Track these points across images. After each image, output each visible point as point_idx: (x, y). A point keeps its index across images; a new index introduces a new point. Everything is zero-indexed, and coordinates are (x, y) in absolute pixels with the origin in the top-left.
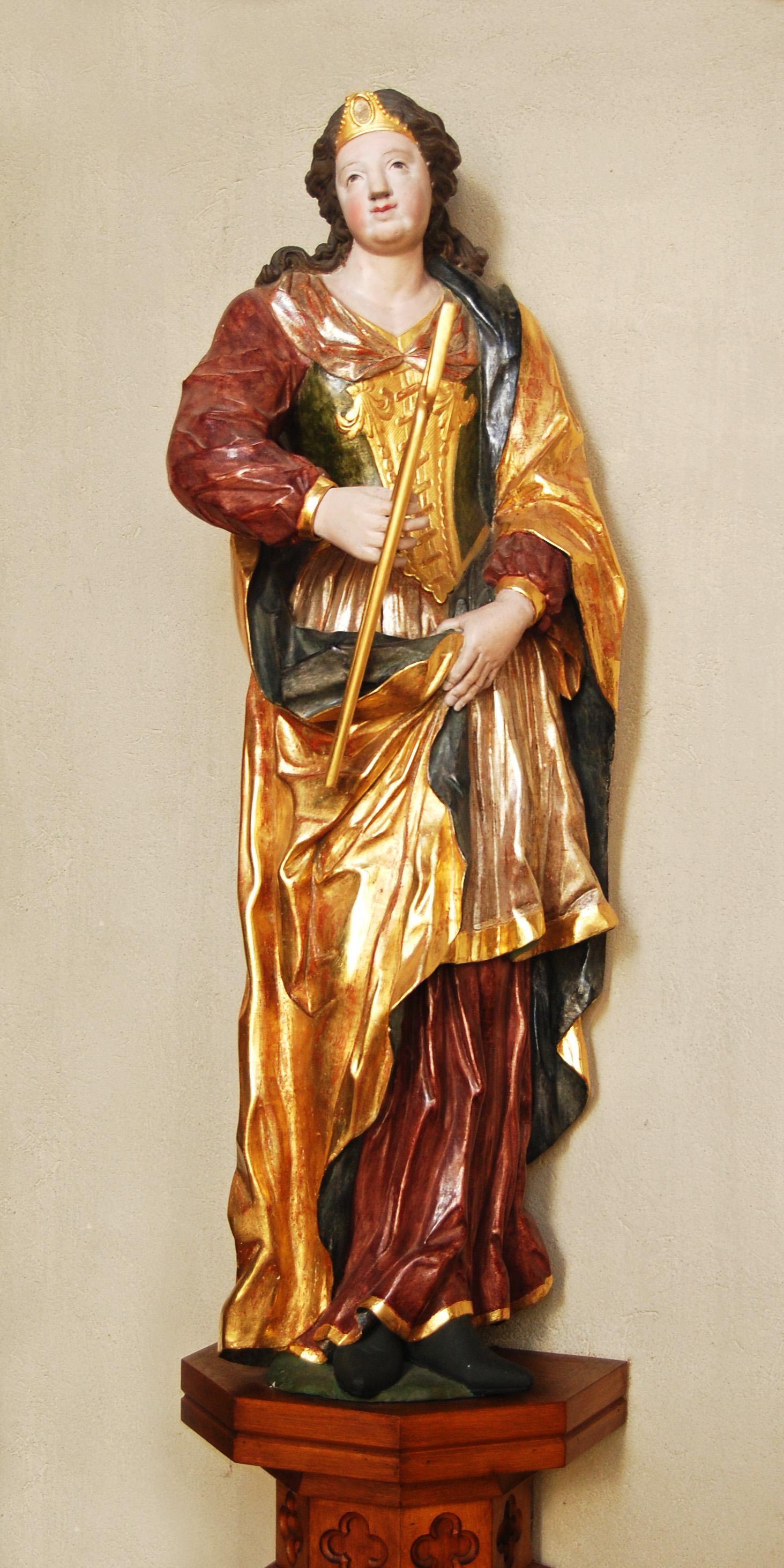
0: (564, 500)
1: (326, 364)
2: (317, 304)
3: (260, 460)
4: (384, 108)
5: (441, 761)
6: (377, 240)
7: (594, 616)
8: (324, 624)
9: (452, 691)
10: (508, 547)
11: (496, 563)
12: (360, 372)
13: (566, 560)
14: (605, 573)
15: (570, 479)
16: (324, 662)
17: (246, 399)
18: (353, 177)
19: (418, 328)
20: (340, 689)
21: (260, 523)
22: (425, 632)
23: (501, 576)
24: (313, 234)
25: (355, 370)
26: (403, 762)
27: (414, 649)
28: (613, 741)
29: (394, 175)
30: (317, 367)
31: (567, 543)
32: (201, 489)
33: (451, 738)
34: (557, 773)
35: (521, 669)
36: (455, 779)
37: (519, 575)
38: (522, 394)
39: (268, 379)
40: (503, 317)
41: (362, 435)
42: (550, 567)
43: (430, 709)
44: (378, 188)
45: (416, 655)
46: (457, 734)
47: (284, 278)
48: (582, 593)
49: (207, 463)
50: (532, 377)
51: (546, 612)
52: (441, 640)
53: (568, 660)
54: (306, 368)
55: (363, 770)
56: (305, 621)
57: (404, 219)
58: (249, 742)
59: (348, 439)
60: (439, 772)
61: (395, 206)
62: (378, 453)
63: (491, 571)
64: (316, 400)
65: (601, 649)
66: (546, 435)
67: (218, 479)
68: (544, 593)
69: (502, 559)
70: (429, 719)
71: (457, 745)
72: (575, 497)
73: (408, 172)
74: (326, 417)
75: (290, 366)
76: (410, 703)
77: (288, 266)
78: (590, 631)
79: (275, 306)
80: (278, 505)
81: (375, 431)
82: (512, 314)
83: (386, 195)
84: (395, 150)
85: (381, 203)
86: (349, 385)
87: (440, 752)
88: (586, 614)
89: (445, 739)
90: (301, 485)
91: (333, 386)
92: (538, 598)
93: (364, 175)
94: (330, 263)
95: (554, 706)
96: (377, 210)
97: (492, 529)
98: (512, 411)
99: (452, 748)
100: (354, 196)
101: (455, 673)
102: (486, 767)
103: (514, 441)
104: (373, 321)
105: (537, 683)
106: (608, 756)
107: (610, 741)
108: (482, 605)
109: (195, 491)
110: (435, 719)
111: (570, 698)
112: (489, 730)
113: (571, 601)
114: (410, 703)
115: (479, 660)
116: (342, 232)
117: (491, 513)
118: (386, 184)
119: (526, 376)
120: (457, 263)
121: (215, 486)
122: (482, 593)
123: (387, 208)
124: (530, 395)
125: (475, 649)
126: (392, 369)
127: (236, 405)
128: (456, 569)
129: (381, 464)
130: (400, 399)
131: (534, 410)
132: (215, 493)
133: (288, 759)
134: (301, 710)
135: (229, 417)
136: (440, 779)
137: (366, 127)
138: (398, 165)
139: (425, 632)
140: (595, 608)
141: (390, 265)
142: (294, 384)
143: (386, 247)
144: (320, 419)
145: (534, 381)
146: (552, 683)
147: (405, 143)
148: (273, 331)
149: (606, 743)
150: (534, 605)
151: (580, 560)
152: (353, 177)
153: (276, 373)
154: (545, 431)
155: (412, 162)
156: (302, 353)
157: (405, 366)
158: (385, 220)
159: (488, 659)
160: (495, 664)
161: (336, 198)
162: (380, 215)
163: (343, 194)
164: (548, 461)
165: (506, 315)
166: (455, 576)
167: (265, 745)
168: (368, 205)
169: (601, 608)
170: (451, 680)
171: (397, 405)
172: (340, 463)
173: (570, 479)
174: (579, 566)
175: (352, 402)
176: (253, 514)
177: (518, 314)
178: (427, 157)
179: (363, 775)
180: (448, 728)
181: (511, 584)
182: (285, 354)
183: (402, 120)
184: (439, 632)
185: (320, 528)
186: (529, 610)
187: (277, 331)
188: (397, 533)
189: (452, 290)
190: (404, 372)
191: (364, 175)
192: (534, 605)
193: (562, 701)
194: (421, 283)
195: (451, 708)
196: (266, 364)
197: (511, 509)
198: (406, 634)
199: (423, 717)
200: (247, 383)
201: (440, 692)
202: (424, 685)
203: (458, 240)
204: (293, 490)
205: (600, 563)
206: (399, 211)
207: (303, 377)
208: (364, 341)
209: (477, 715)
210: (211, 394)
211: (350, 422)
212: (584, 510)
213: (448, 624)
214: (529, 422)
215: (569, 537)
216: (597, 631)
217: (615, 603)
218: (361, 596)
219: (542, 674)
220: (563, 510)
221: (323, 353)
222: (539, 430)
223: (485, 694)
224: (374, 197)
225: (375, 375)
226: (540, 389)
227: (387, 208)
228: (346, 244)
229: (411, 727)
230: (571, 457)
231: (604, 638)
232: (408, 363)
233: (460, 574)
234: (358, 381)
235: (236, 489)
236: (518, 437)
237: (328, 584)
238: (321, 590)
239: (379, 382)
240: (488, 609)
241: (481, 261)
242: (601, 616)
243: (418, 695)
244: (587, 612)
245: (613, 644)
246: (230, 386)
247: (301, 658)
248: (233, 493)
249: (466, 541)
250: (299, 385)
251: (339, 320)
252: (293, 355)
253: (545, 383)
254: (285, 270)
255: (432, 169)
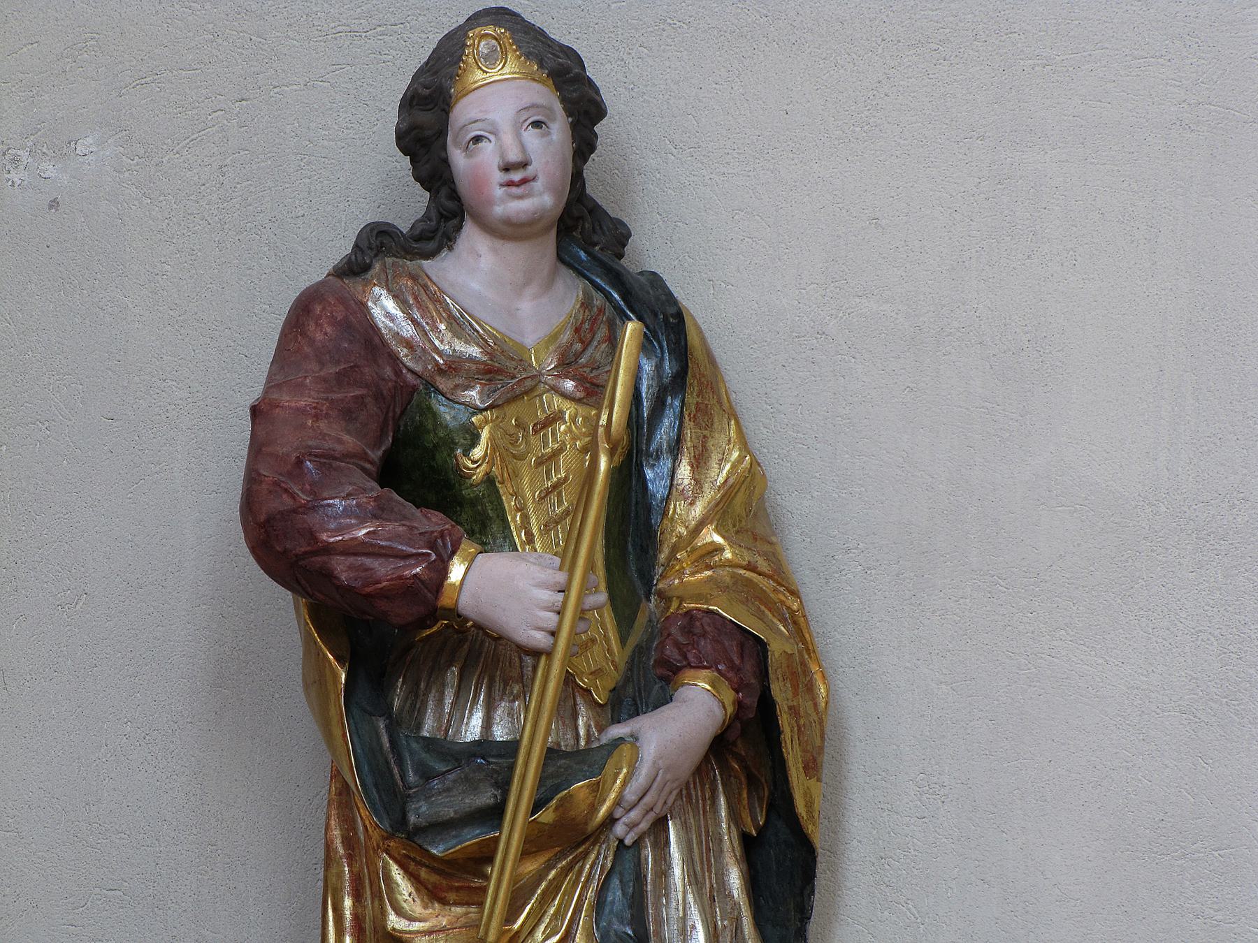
0: (751, 567)
1: (443, 384)
2: (423, 299)
3: (384, 516)
4: (519, 48)
5: (611, 912)
6: (508, 222)
7: (793, 722)
8: (447, 731)
9: (624, 819)
10: (682, 628)
11: (671, 651)
12: (489, 397)
13: (761, 646)
14: (803, 663)
15: (755, 539)
16: (467, 779)
17: (349, 432)
18: (477, 139)
19: (554, 337)
20: (494, 815)
21: (387, 598)
22: (582, 743)
23: (677, 670)
24: (408, 205)
25: (481, 393)
26: (560, 914)
27: (577, 763)
28: (813, 892)
29: (532, 138)
30: (431, 386)
31: (760, 625)
32: (305, 553)
33: (621, 882)
34: (742, 932)
35: (696, 794)
36: (630, 932)
37: (705, 668)
38: (688, 424)
39: (372, 408)
40: (669, 325)
41: (489, 480)
42: (742, 657)
43: (594, 844)
44: (514, 156)
45: (582, 770)
46: (629, 876)
47: (377, 266)
48: (780, 692)
49: (313, 520)
50: (699, 400)
51: (736, 717)
52: (610, 754)
53: (752, 782)
54: (414, 389)
55: (514, 922)
56: (419, 726)
57: (541, 199)
58: (331, 891)
59: (472, 485)
60: (610, 923)
61: (534, 179)
62: (509, 504)
63: (663, 662)
64: (428, 432)
65: (800, 765)
66: (721, 480)
67: (332, 540)
68: (737, 692)
69: (677, 645)
70: (593, 856)
71: (631, 890)
72: (765, 564)
73: (548, 134)
74: (441, 456)
75: (395, 388)
76: (567, 838)
77: (380, 251)
78: (789, 742)
79: (376, 312)
80: (415, 575)
81: (506, 475)
82: (672, 315)
83: (524, 165)
84: (533, 106)
85: (516, 176)
86: (473, 414)
87: (610, 898)
88: (784, 721)
89: (615, 882)
90: (443, 552)
91: (447, 414)
92: (729, 696)
93: (492, 137)
94: (431, 245)
95: (736, 844)
96: (510, 184)
97: (652, 605)
98: (676, 449)
99: (624, 894)
100: (476, 165)
101: (630, 796)
102: (659, 922)
103: (681, 488)
104: (494, 325)
105: (715, 811)
106: (804, 913)
107: (806, 892)
108: (656, 707)
109: (296, 556)
110: (599, 859)
111: (754, 833)
112: (663, 871)
113: (766, 705)
114: (567, 838)
115: (659, 779)
116: (450, 205)
117: (648, 583)
118: (523, 148)
119: (691, 399)
120: (596, 245)
121: (328, 549)
122: (654, 692)
123: (524, 181)
124: (697, 425)
125: (654, 763)
126: (526, 393)
127: (340, 441)
128: (616, 659)
129: (514, 518)
130: (536, 432)
131: (704, 446)
132: (325, 558)
133: (400, 912)
134: (432, 843)
135: (335, 459)
136: (612, 933)
137: (495, 74)
138: (537, 124)
139: (582, 743)
140: (794, 711)
141: (516, 255)
142: (398, 411)
143: (510, 231)
144: (434, 458)
145: (702, 406)
146: (734, 816)
147: (543, 95)
148: (371, 340)
149: (802, 893)
150: (724, 707)
151: (778, 648)
152: (477, 139)
153: (378, 396)
154: (720, 474)
155: (553, 120)
156: (409, 370)
157: (542, 387)
158: (520, 197)
159: (668, 777)
160: (675, 785)
161: (446, 162)
162: (514, 190)
163: (459, 159)
164: (721, 513)
165: (666, 317)
166: (616, 668)
167: (357, 896)
168: (498, 176)
169: (802, 713)
170: (625, 804)
171: (533, 440)
172: (480, 520)
173: (755, 539)
174: (777, 655)
175: (478, 436)
176: (379, 586)
177: (680, 316)
178: (569, 113)
179: (516, 926)
180: (618, 869)
181: (696, 678)
182: (388, 372)
183: (541, 66)
184: (604, 740)
185: (466, 604)
186: (719, 713)
187: (376, 340)
188: (575, 614)
189: (592, 282)
190: (541, 396)
191: (492, 137)
192: (724, 707)
193: (746, 840)
194: (553, 275)
195: (621, 841)
196: (367, 386)
197: (685, 579)
198: (559, 744)
199: (586, 855)
200: (348, 414)
201: (611, 820)
202: (594, 809)
203: (595, 210)
204: (434, 557)
205: (800, 652)
206: (538, 185)
207: (410, 402)
208: (491, 355)
209: (648, 854)
210: (303, 426)
211: (474, 462)
212: (774, 581)
213: (617, 731)
214: (699, 463)
215: (761, 617)
216: (796, 741)
217: (815, 705)
218: (497, 694)
219: (722, 801)
220: (749, 580)
221: (440, 371)
222: (713, 472)
223: (660, 825)
224: (507, 168)
225: (509, 401)
226: (711, 417)
227: (524, 181)
228: (455, 222)
229: (570, 868)
230: (745, 508)
231: (805, 751)
232: (546, 383)
233: (622, 667)
234: (486, 409)
235: (356, 554)
236: (686, 482)
237: (453, 674)
238: (443, 686)
239: (512, 410)
240: (667, 711)
241: (620, 236)
242: (802, 721)
243: (586, 824)
244: (785, 716)
245: (815, 760)
246: (327, 416)
247: (427, 775)
248: (351, 559)
249: (625, 622)
250: (402, 413)
251: (458, 326)
252: (398, 373)
253: (717, 408)
254: (376, 255)
255: (574, 126)
